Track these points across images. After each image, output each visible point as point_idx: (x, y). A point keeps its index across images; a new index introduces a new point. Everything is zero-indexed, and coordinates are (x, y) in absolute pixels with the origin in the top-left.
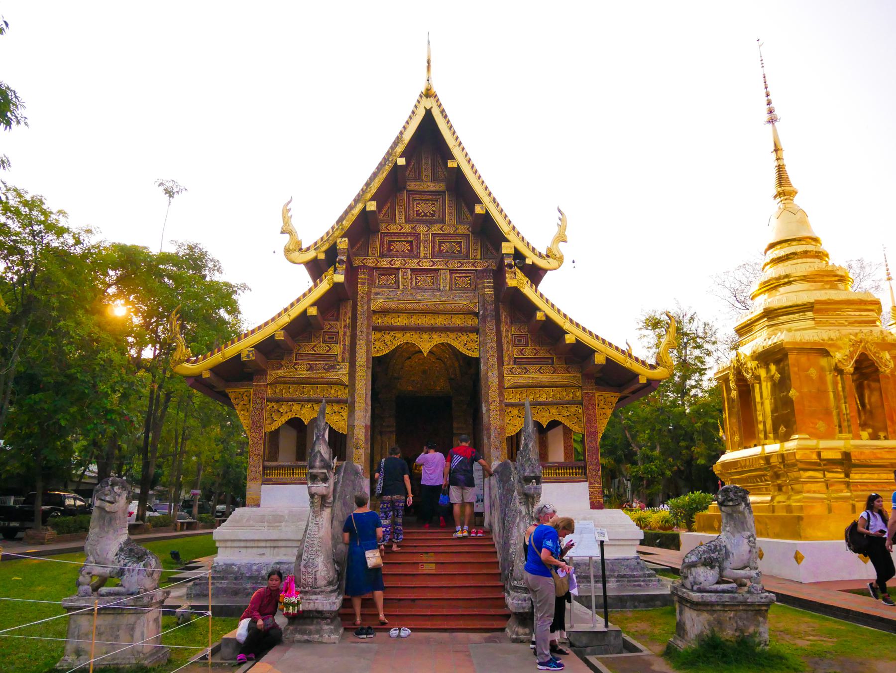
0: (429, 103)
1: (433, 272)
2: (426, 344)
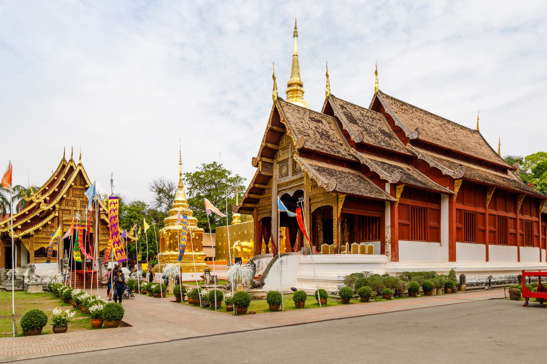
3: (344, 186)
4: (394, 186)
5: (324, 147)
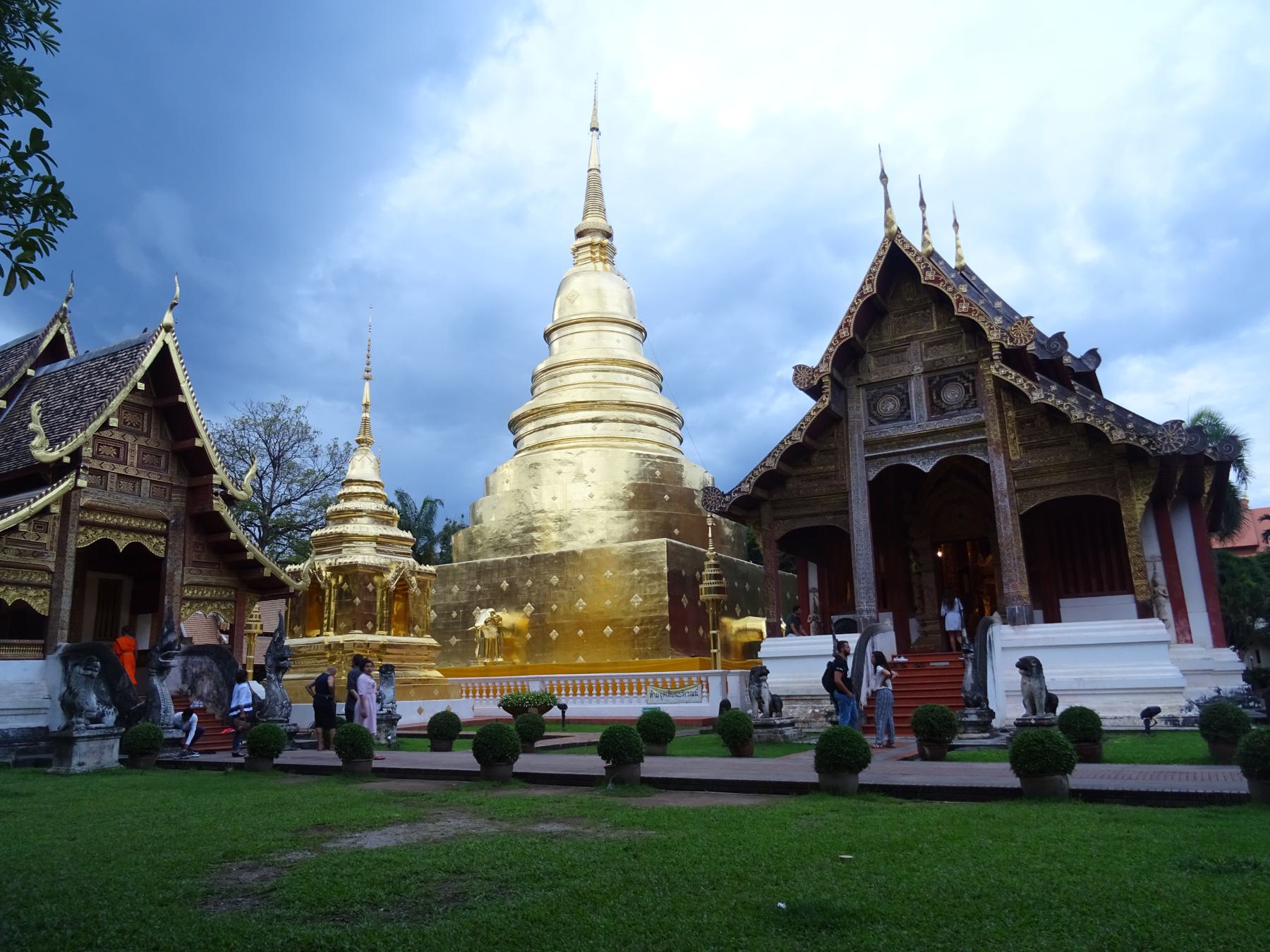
2: (122, 542)
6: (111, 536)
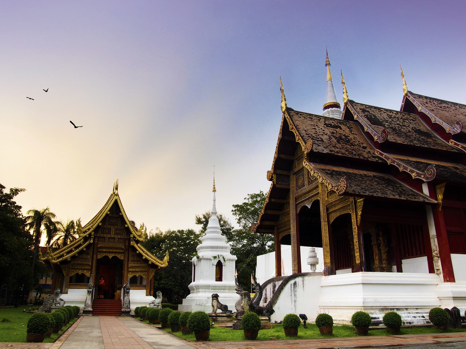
0: (116, 197)
1: (114, 238)
2: (111, 256)
3: (362, 189)
4: (432, 186)
5: (340, 150)
6: (106, 254)
